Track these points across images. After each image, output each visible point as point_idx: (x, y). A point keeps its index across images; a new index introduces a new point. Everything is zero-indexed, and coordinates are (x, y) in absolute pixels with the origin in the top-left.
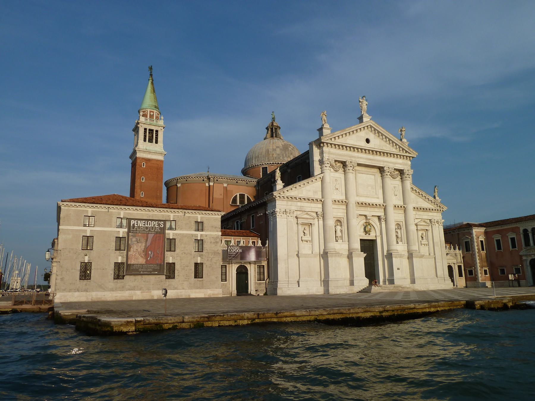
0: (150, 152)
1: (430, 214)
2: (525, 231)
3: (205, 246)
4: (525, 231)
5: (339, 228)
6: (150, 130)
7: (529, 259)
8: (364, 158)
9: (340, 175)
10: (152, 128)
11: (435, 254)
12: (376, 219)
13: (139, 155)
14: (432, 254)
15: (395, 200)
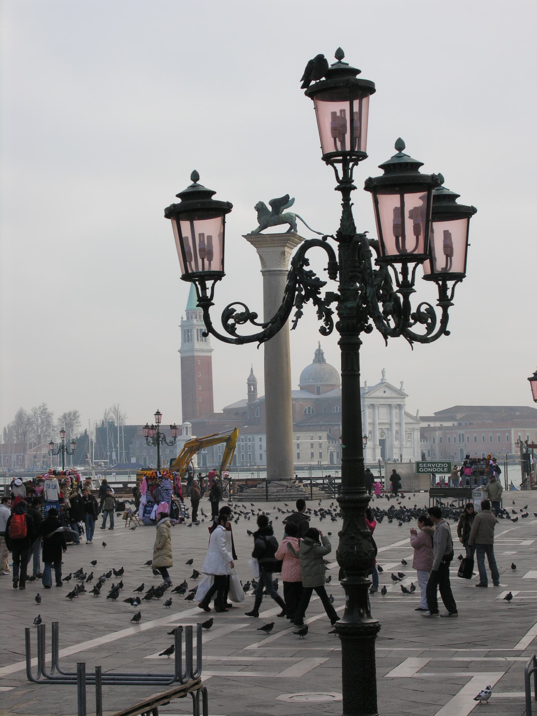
0: (203, 351)
1: (414, 425)
2: (460, 434)
3: (322, 445)
4: (460, 434)
5: (370, 435)
6: (200, 329)
7: (460, 448)
8: (382, 401)
9: (371, 410)
10: (201, 328)
11: (414, 445)
12: (386, 430)
13: (196, 354)
14: (412, 446)
15: (395, 420)
